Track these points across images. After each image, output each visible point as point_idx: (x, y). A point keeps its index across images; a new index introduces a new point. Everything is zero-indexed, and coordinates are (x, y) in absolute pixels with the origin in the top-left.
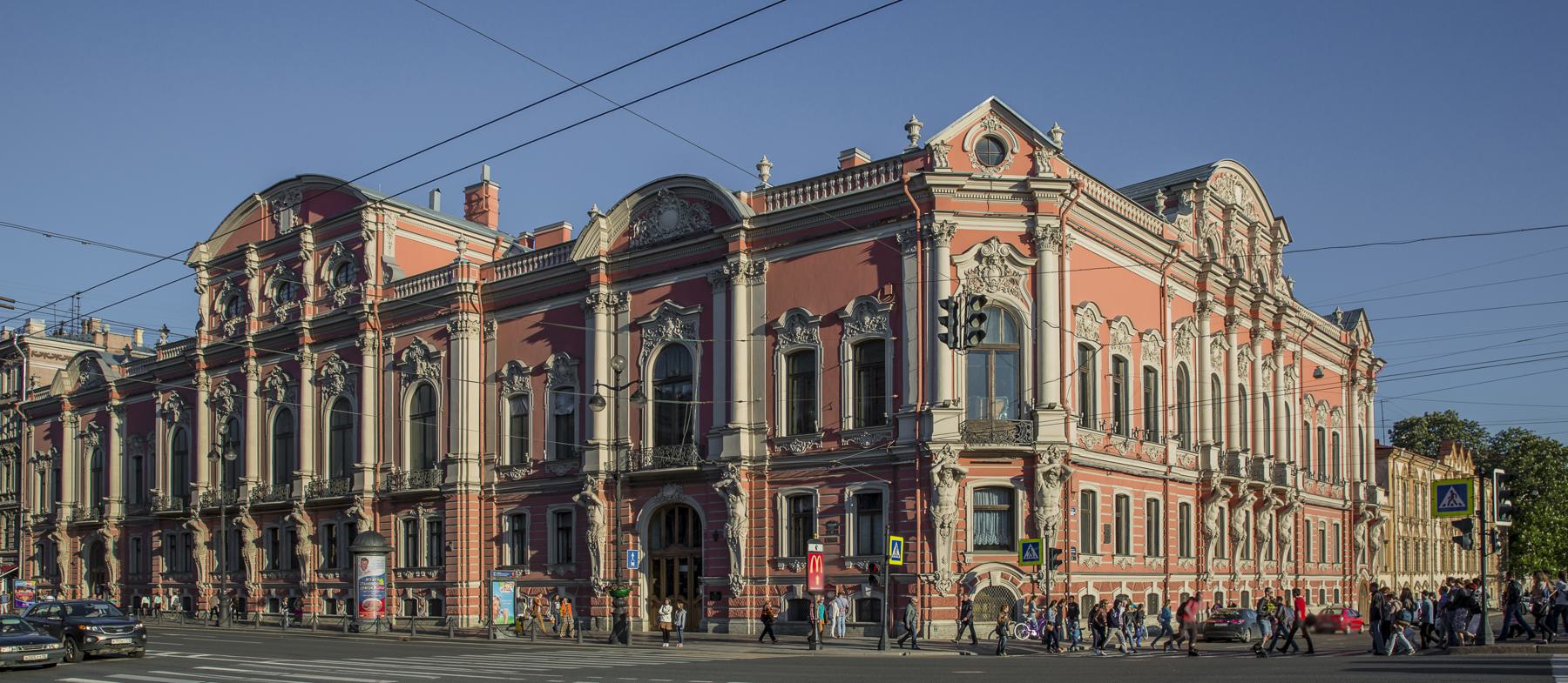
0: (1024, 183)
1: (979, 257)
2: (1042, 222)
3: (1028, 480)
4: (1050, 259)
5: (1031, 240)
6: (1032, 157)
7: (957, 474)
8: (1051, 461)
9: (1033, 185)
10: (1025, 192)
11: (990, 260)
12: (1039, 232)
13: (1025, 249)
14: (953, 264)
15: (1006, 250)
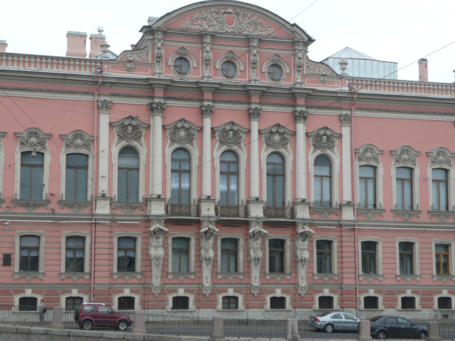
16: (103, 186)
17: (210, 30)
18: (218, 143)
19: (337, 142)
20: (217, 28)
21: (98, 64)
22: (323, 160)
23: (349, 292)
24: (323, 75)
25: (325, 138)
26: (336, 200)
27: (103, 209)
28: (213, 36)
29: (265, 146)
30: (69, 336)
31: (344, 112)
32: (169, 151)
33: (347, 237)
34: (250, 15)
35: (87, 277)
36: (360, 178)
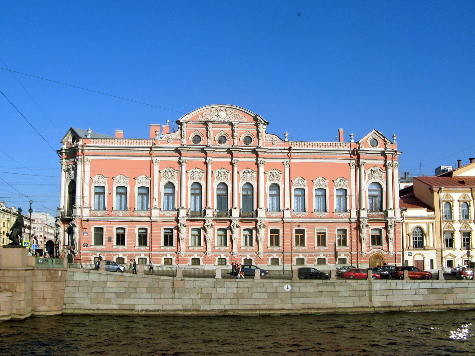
0: (383, 152)
1: (372, 170)
2: (388, 161)
3: (386, 228)
4: (390, 170)
5: (385, 165)
6: (385, 144)
7: (367, 226)
8: (391, 223)
9: (386, 152)
10: (383, 154)
11: (374, 171)
12: (387, 164)
13: (384, 168)
14: (365, 172)
15: (379, 169)
16: (156, 203)
17: (212, 120)
18: (216, 179)
19: (281, 176)
20: (215, 118)
21: (154, 141)
22: (275, 187)
23: (287, 256)
24: (274, 141)
25: (275, 174)
26: (282, 208)
27: (155, 213)
28: (213, 122)
29: (241, 179)
30: (107, 274)
31: (286, 160)
32: (190, 183)
33: (287, 227)
34: (234, 111)
35: (148, 248)
36: (295, 195)
